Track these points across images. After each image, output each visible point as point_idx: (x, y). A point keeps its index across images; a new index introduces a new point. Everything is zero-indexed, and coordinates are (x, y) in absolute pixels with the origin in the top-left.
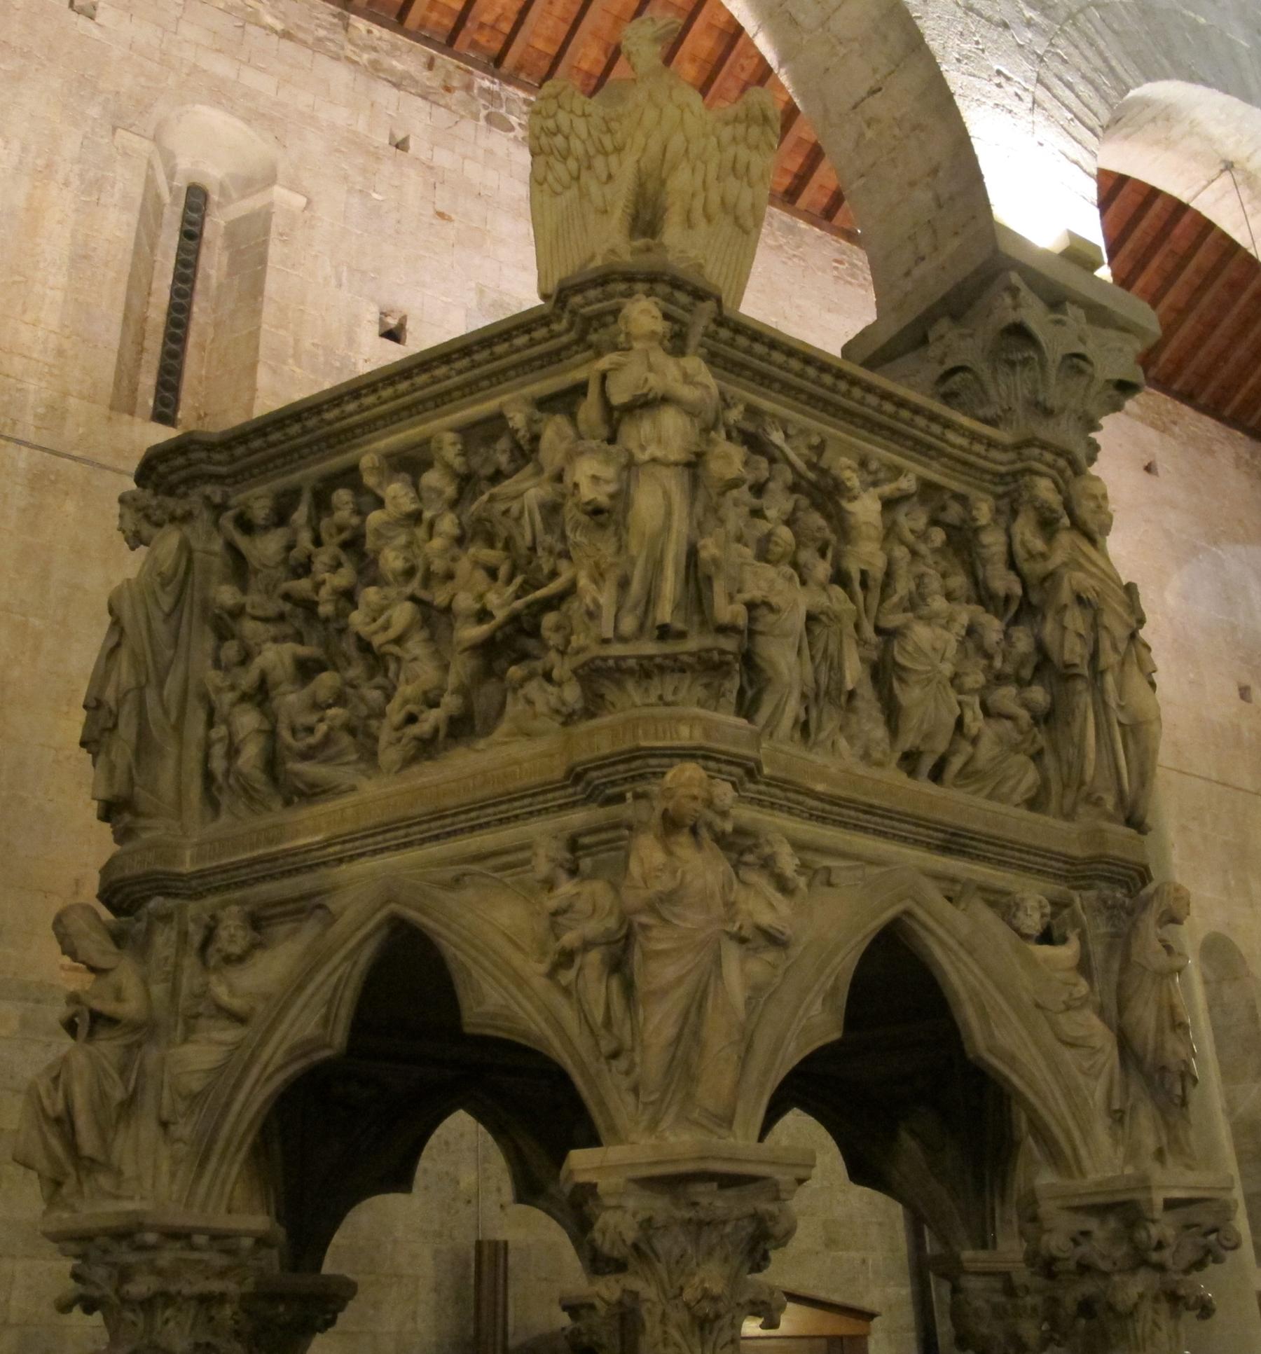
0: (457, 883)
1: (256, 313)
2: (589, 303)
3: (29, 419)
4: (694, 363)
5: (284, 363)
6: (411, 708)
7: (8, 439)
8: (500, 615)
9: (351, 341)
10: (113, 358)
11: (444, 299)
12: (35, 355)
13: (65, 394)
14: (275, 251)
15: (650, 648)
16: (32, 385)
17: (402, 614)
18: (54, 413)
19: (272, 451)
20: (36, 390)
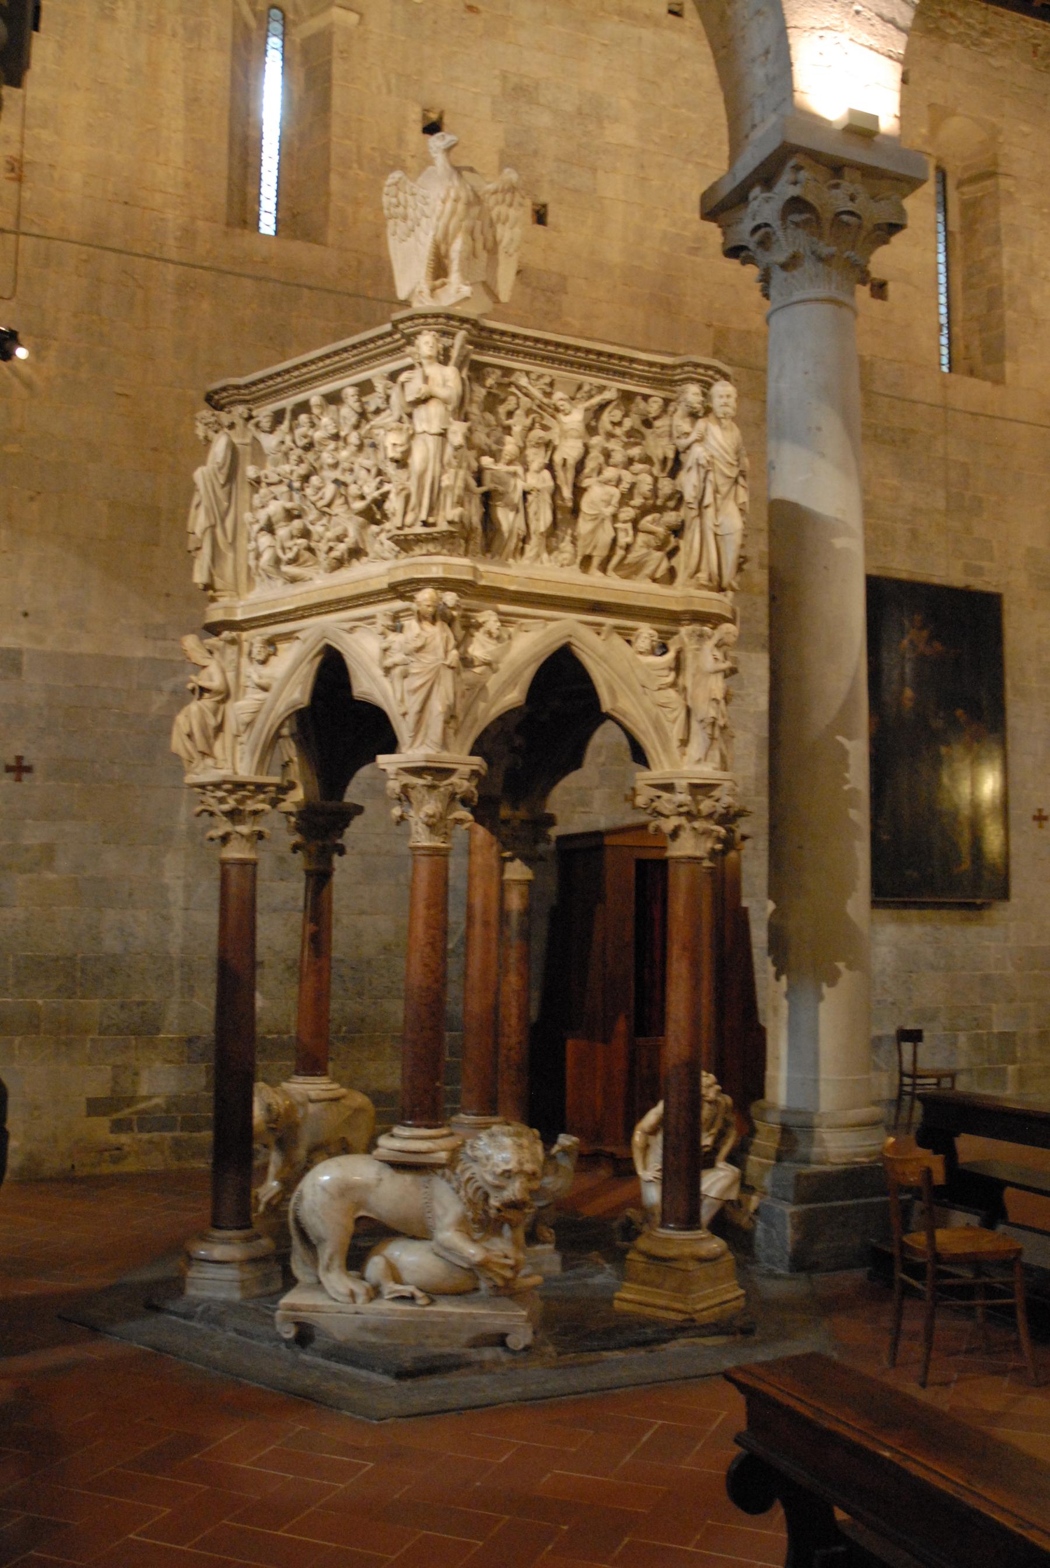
0: (351, 630)
1: (326, 126)
2: (407, 328)
3: (171, 242)
4: (450, 372)
5: (350, 168)
6: (331, 544)
7: (157, 259)
8: (369, 498)
9: (401, 141)
10: (224, 183)
11: (474, 90)
12: (170, 190)
13: (193, 218)
14: (338, 69)
15: (419, 529)
16: (170, 214)
17: (330, 490)
18: (188, 234)
19: (269, 390)
20: (174, 218)
